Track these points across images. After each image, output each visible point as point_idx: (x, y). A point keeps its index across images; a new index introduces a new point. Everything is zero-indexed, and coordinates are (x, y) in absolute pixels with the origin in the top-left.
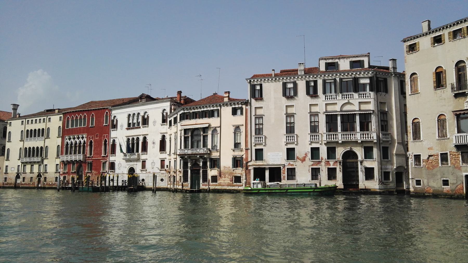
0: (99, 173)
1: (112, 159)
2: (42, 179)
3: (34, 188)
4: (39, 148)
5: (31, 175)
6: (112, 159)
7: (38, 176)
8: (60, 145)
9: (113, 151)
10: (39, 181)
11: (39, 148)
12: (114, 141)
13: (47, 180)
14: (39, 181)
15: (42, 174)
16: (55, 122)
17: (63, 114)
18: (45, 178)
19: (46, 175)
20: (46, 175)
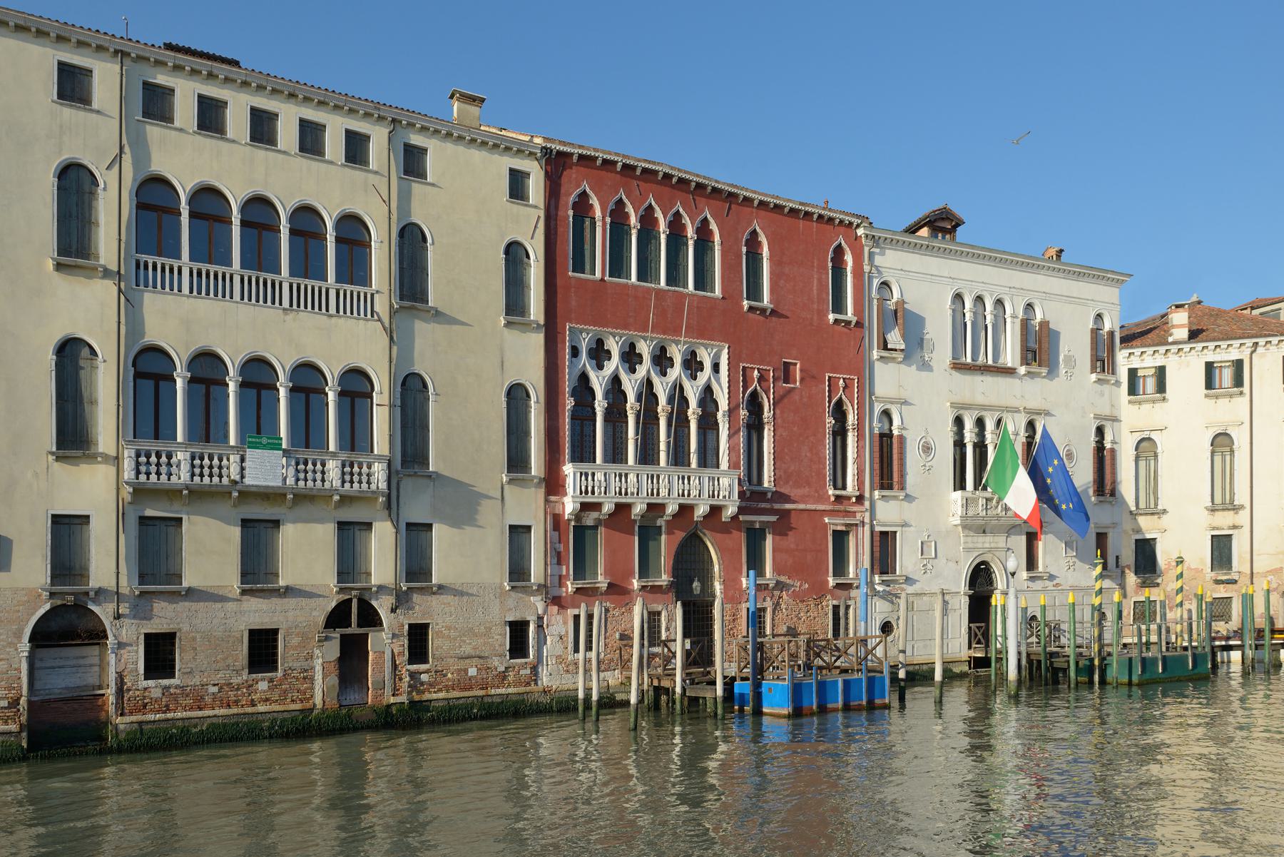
0: (819, 591)
1: (888, 512)
2: (385, 644)
3: (300, 729)
4: (332, 372)
5: (259, 613)
6: (888, 512)
7: (337, 618)
8: (535, 381)
9: (887, 471)
10: (352, 658)
11: (332, 372)
12: (887, 414)
13: (434, 643)
14: (352, 658)
15: (382, 606)
16: (475, 210)
17: (556, 163)
18: (418, 638)
19: (425, 609)
20: (425, 609)
